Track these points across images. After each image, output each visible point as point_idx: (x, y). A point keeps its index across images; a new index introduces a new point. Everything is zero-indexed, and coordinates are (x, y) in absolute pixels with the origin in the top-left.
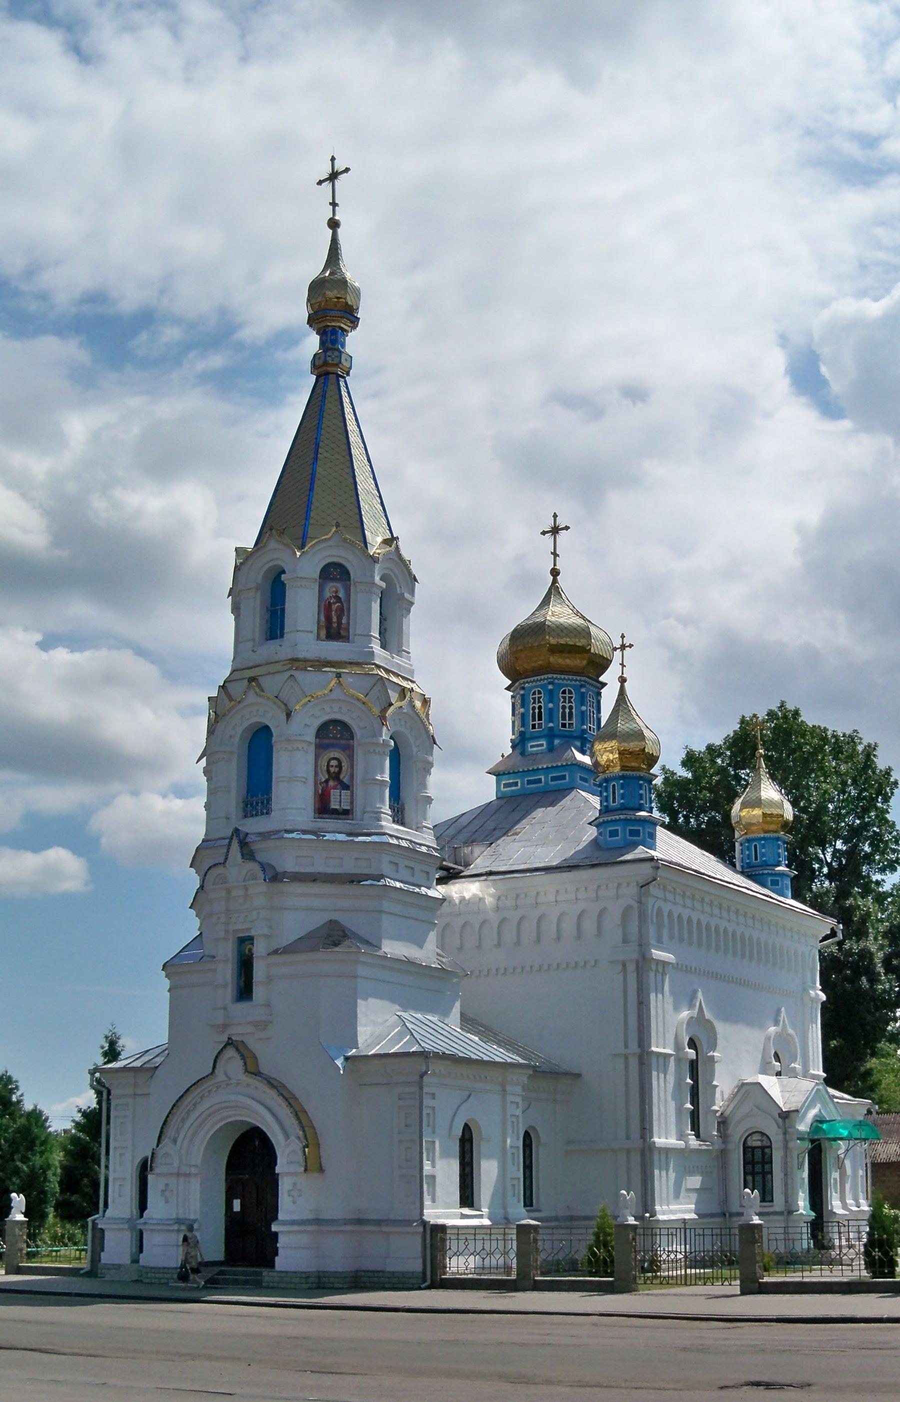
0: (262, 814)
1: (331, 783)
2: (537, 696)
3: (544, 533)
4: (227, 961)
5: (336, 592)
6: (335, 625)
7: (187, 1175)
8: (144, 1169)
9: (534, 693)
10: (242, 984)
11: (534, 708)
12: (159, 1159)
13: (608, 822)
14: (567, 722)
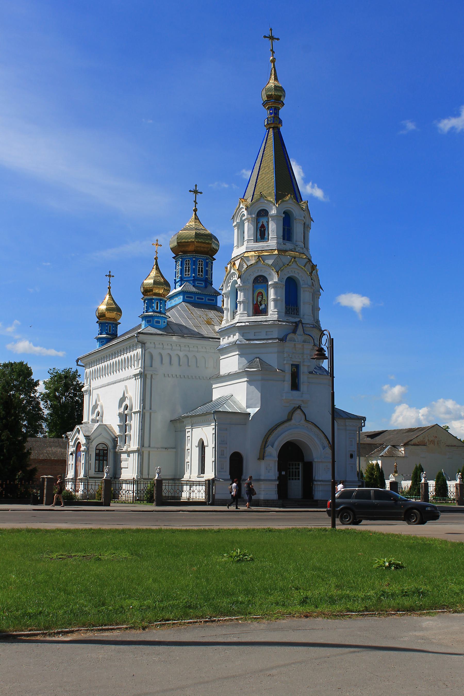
9: (186, 261)
11: (186, 267)
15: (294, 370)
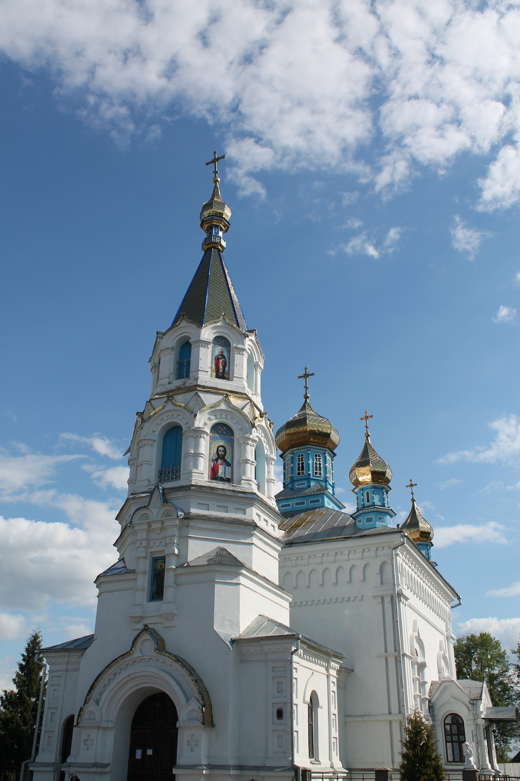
0: (172, 479)
1: (220, 461)
2: (301, 457)
3: (300, 377)
4: (145, 573)
5: (222, 352)
6: (221, 371)
7: (105, 729)
8: (69, 725)
9: (299, 456)
10: (154, 589)
11: (299, 464)
12: (86, 715)
13: (366, 513)
14: (318, 472)
15: (161, 566)
